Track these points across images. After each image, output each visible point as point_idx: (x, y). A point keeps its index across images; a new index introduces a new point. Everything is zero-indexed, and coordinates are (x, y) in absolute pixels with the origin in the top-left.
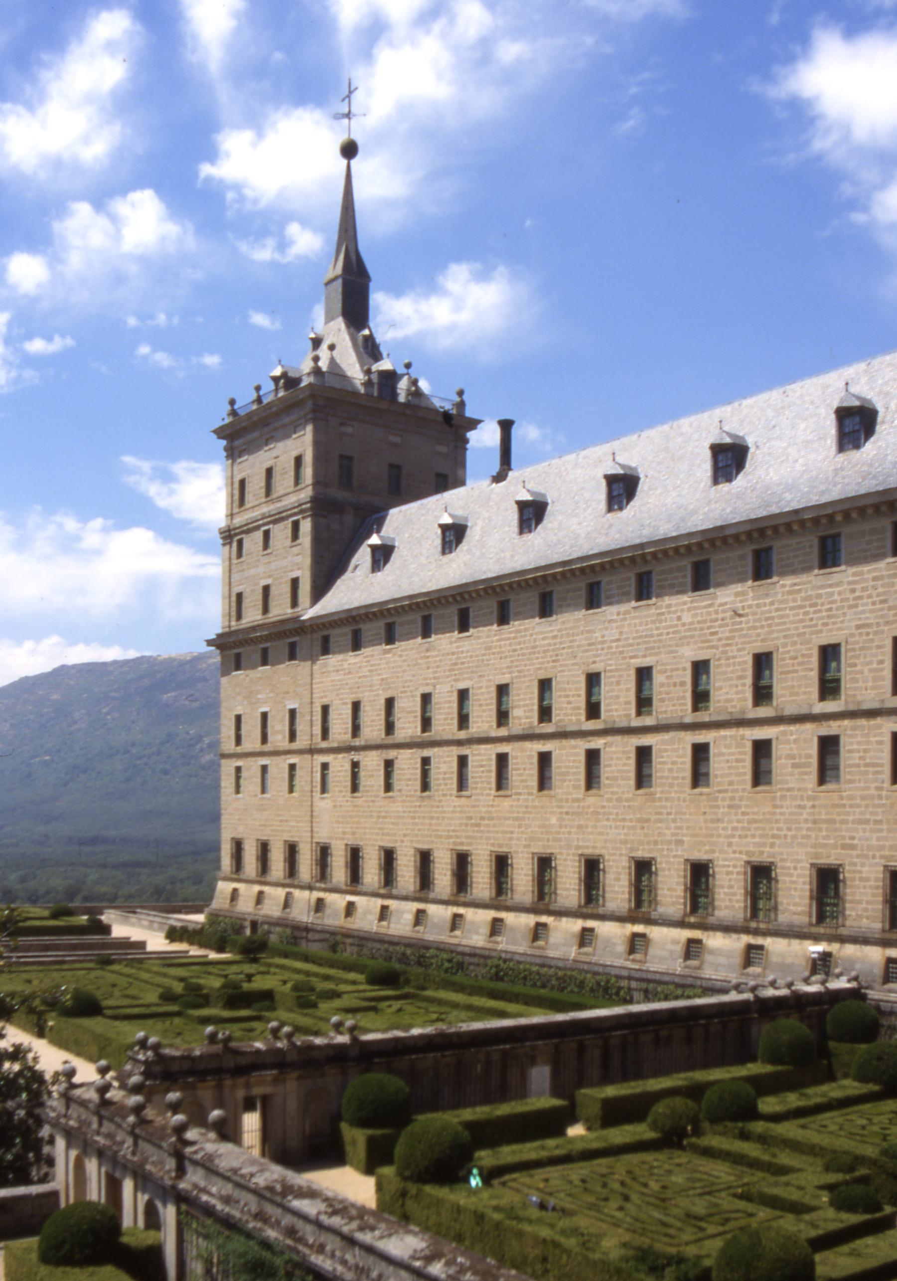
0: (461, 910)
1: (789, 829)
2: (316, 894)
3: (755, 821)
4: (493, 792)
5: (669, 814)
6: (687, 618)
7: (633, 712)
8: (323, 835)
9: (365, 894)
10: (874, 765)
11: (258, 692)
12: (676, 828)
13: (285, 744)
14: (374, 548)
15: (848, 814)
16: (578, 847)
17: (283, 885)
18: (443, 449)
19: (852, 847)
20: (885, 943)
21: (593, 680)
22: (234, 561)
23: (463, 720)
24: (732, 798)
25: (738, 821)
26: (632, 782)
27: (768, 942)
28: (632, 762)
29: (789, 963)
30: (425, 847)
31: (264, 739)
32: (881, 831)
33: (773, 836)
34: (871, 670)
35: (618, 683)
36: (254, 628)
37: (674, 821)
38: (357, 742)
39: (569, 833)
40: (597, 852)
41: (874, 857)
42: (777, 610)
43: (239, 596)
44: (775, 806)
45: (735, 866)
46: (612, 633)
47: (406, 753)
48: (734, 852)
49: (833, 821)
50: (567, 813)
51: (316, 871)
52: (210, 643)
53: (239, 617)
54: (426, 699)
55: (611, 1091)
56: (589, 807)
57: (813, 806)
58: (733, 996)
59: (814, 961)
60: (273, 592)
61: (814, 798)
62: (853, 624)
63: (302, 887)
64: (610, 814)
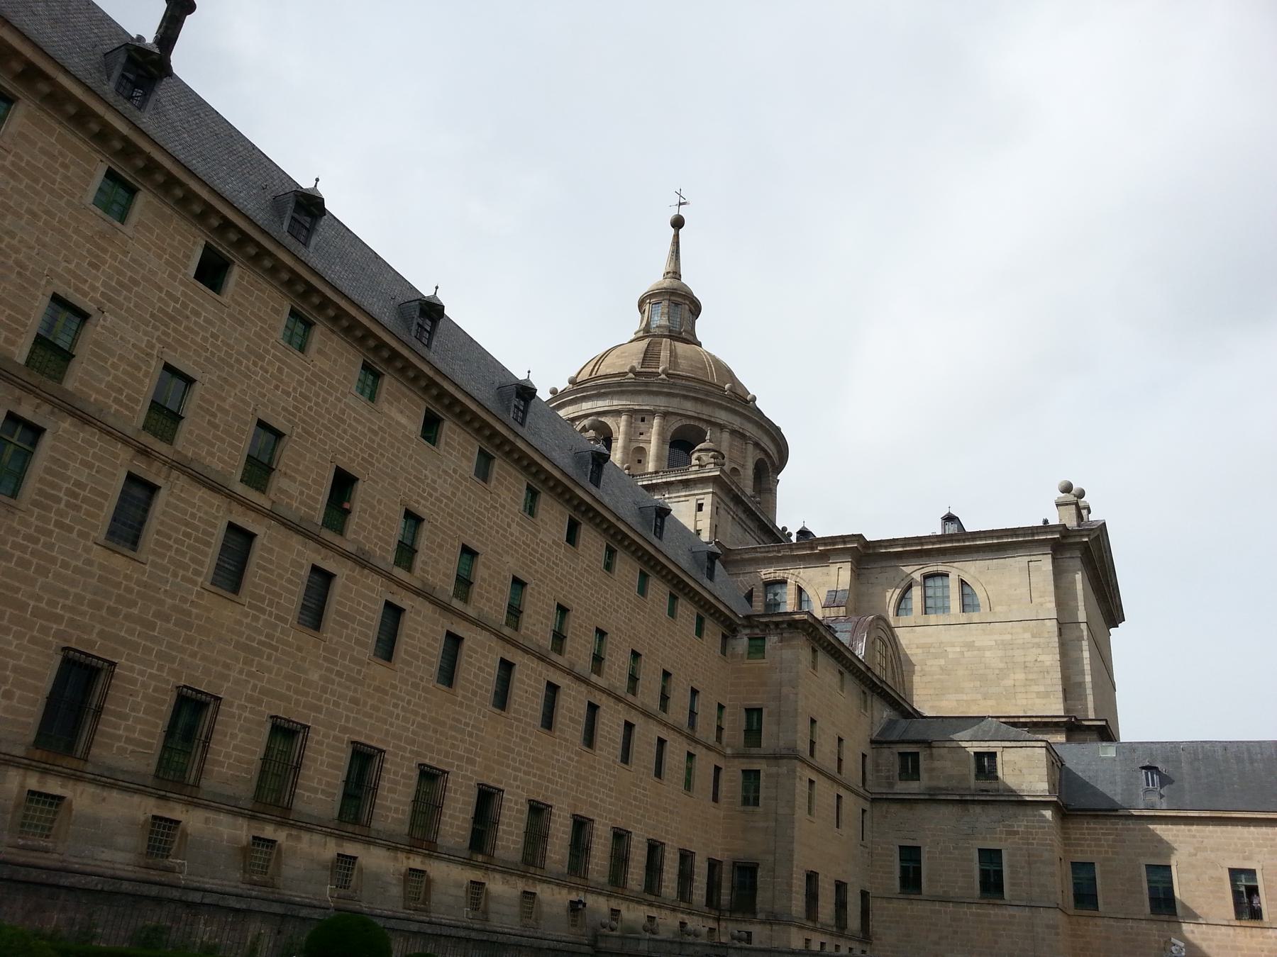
1: (560, 777)
5: (467, 724)
19: (596, 806)
33: (549, 780)
37: (470, 735)
39: (336, 704)
45: (516, 803)
48: (518, 787)
50: (339, 674)
61: (579, 754)
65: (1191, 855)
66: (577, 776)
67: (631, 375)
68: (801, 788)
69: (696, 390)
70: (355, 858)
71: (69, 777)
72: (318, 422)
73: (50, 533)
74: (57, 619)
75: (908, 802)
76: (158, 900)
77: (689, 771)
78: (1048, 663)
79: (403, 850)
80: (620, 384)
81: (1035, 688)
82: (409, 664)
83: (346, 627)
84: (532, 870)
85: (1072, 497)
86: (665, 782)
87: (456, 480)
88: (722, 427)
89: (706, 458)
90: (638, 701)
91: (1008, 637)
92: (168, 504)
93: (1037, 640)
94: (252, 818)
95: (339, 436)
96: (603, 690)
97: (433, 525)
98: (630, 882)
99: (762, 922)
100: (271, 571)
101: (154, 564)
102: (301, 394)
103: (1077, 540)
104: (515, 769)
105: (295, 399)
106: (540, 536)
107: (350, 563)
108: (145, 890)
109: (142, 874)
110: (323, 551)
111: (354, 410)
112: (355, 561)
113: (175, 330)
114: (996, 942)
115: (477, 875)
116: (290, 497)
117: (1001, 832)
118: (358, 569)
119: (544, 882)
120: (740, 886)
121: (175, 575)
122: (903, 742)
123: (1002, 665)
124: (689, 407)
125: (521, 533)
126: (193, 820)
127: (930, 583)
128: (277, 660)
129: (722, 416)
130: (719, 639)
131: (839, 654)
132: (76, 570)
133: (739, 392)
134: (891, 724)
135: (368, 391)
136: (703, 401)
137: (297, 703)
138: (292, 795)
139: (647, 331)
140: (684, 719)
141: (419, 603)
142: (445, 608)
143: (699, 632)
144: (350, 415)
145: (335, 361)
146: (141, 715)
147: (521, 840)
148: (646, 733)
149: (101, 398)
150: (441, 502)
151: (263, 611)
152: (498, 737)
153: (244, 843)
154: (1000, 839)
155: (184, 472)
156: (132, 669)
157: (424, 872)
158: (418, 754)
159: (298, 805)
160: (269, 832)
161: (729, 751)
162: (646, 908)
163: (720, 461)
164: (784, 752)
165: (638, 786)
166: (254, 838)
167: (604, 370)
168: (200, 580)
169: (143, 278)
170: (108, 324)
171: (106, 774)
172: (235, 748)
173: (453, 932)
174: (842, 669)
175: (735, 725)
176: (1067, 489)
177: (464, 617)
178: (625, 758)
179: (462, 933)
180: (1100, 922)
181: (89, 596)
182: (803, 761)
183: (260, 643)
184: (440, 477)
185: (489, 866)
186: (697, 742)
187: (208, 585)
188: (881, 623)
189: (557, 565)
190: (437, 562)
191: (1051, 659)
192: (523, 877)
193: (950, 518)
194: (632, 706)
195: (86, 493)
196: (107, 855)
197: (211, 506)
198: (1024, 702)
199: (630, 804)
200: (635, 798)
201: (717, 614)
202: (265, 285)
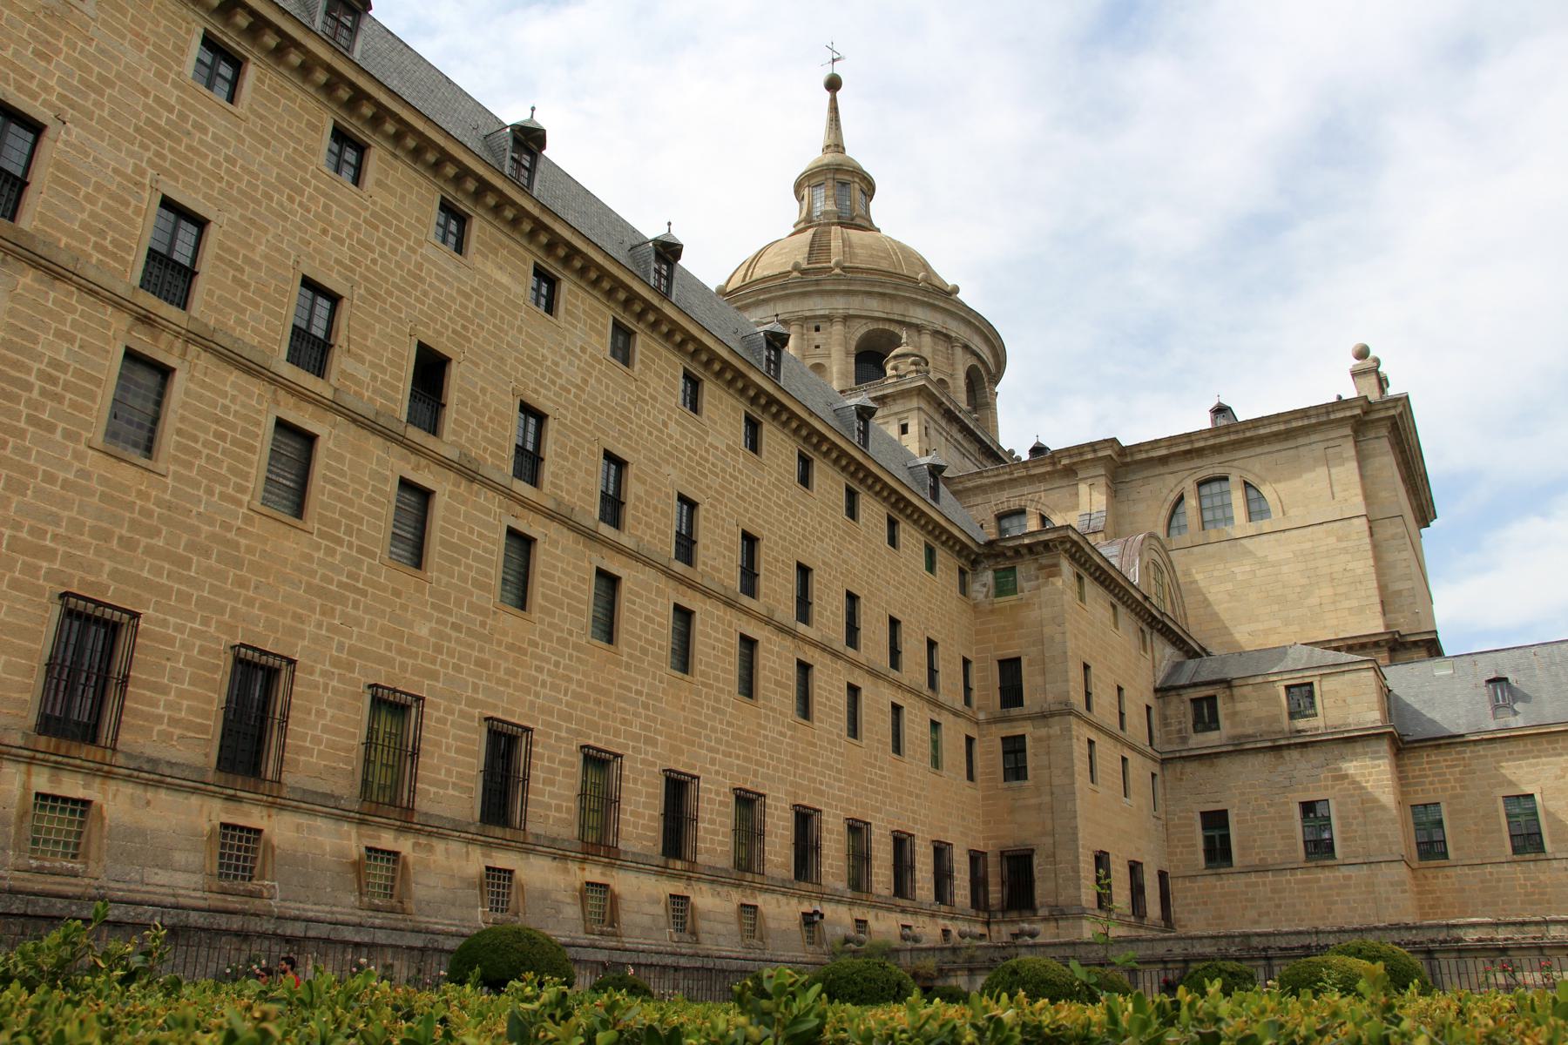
5: (639, 693)
12: (647, 717)
19: (821, 793)
25: (724, 732)
32: (840, 780)
33: (758, 763)
37: (646, 706)
39: (457, 668)
45: (718, 793)
50: (456, 627)
56: (505, 633)
61: (794, 729)
64: (547, 660)
65: (1557, 778)
66: (794, 755)
67: (795, 274)
68: (1080, 750)
69: (882, 284)
70: (511, 872)
71: (92, 773)
72: (386, 280)
73: (21, 434)
74: (50, 554)
75: (1209, 758)
76: (244, 936)
77: (936, 744)
78: (1360, 571)
79: (574, 859)
80: (783, 287)
81: (1346, 604)
82: (551, 613)
83: (458, 563)
84: (749, 876)
85: (1366, 365)
86: (907, 759)
87: (587, 363)
88: (918, 328)
89: (905, 366)
90: (862, 656)
91: (1308, 545)
92: (187, 392)
93: (1344, 544)
94: (362, 822)
95: (417, 299)
96: (814, 644)
97: (561, 424)
98: (875, 885)
99: (1045, 919)
100: (344, 487)
101: (178, 477)
102: (359, 241)
103: (1383, 414)
104: (711, 750)
105: (351, 247)
106: (709, 440)
107: (452, 475)
108: (222, 921)
109: (216, 901)
110: (413, 458)
111: (435, 264)
112: (458, 472)
113: (172, 150)
114: (1329, 911)
115: (678, 888)
116: (358, 383)
117: (1326, 778)
118: (464, 483)
119: (766, 891)
120: (1015, 879)
121: (210, 492)
122: (1195, 685)
123: (1304, 581)
124: (875, 307)
125: (682, 435)
126: (280, 829)
127: (1205, 490)
128: (367, 610)
129: (919, 315)
130: (956, 575)
131: (1107, 579)
132: (66, 484)
133: (937, 283)
134: (1177, 667)
135: (452, 239)
136: (892, 297)
137: (403, 666)
138: (413, 791)
139: (807, 222)
140: (922, 678)
141: (554, 529)
142: (591, 536)
143: (931, 567)
144: (429, 273)
145: (403, 197)
146: (186, 686)
147: (730, 840)
148: (877, 700)
149: (74, 243)
150: (569, 391)
151: (340, 542)
152: (683, 708)
153: (356, 857)
154: (1326, 788)
155: (206, 349)
156: (165, 623)
157: (606, 886)
158: (579, 733)
159: (422, 804)
160: (387, 840)
161: (982, 716)
162: (900, 916)
163: (922, 367)
164: (1053, 708)
165: (874, 766)
166: (369, 849)
167: (759, 273)
168: (246, 498)
169: (119, 76)
170: (73, 139)
171: (146, 767)
172: (325, 729)
173: (655, 959)
174: (1114, 601)
175: (987, 682)
176: (1362, 353)
177: (619, 549)
178: (854, 731)
179: (669, 960)
180: (1448, 871)
181: (89, 522)
182: (1079, 716)
183: (340, 584)
184: (563, 358)
185: (692, 873)
186: (940, 706)
187: (257, 505)
188: (1154, 542)
189: (736, 479)
190: (572, 473)
191: (1363, 565)
192: (739, 886)
193: (1220, 410)
194: (855, 664)
195: (69, 377)
196: (162, 877)
197: (250, 395)
198: (1335, 622)
199: (866, 789)
200: (871, 781)
201: (950, 541)
202: (294, 91)
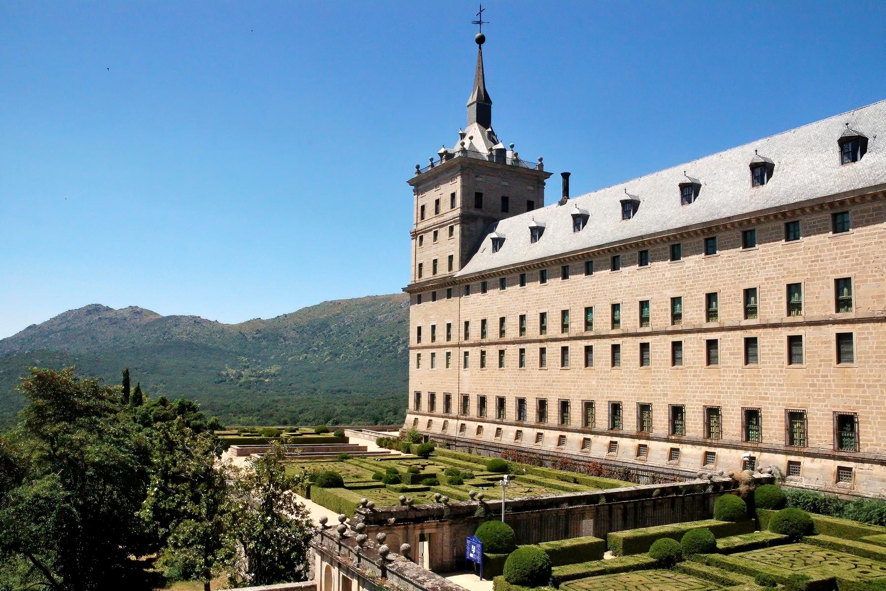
0: (541, 431)
1: (729, 388)
2: (461, 422)
3: (708, 384)
4: (560, 367)
6: (668, 275)
7: (638, 325)
8: (465, 391)
9: (488, 422)
10: (777, 354)
11: (431, 315)
13: (445, 343)
14: (493, 240)
15: (763, 380)
16: (607, 397)
17: (442, 417)
18: (531, 188)
19: (767, 399)
20: (787, 453)
21: (615, 307)
22: (418, 247)
23: (543, 328)
24: (695, 371)
26: (638, 362)
27: (717, 450)
28: (638, 351)
29: (729, 463)
30: (521, 396)
31: (433, 339)
33: (720, 392)
34: (774, 303)
35: (629, 309)
36: (428, 282)
37: (662, 383)
38: (484, 341)
40: (618, 400)
41: (779, 404)
42: (719, 270)
43: (421, 265)
44: (720, 376)
46: (626, 283)
47: (511, 347)
49: (755, 384)
51: (461, 409)
52: (404, 289)
53: (420, 276)
54: (522, 318)
55: (628, 533)
57: (743, 376)
58: (698, 481)
59: (745, 462)
60: (439, 263)
61: (743, 372)
62: (763, 278)
63: (453, 418)
200: (811, 385)
